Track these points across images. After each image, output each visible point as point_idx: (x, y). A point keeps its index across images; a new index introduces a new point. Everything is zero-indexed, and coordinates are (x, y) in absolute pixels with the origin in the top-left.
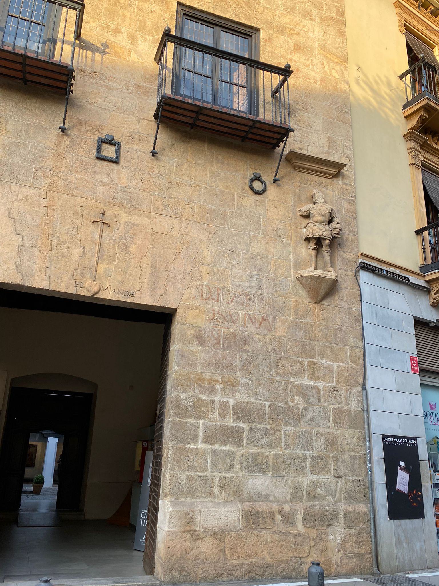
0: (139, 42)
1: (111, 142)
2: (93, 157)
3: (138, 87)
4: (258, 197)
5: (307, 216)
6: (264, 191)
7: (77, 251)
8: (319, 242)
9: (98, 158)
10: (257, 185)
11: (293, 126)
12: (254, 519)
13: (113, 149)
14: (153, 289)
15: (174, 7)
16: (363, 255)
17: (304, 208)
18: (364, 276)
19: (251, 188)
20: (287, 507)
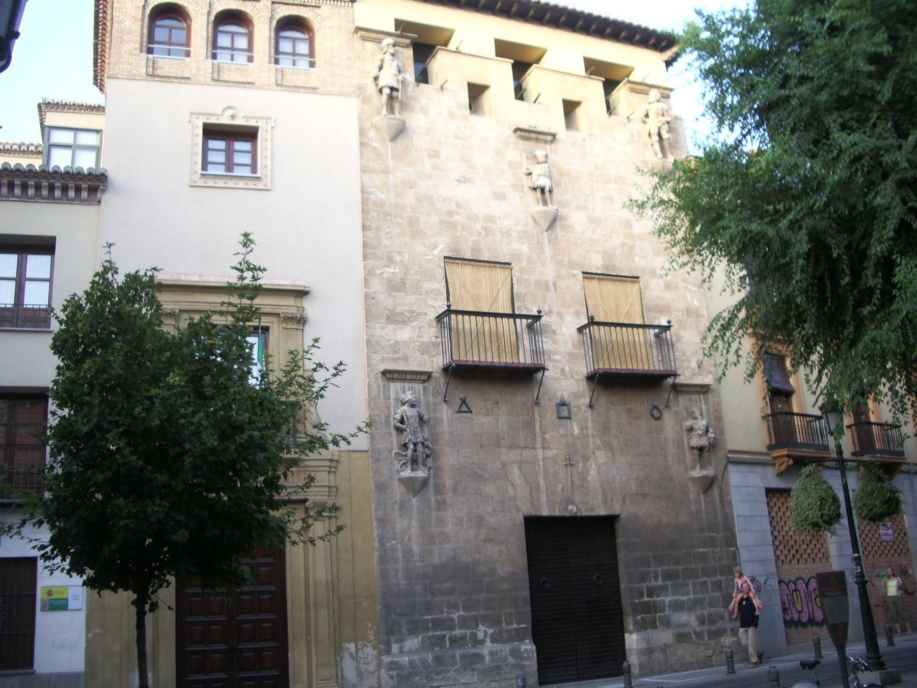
0: (565, 316)
1: (563, 404)
2: (555, 417)
3: (571, 354)
4: (657, 422)
5: (691, 429)
6: (661, 416)
7: (559, 487)
8: (701, 449)
9: (559, 418)
10: (655, 413)
11: (679, 372)
12: (681, 638)
13: (566, 407)
14: (605, 502)
15: (581, 275)
16: (731, 452)
17: (689, 423)
18: (731, 468)
19: (653, 416)
20: (698, 629)
